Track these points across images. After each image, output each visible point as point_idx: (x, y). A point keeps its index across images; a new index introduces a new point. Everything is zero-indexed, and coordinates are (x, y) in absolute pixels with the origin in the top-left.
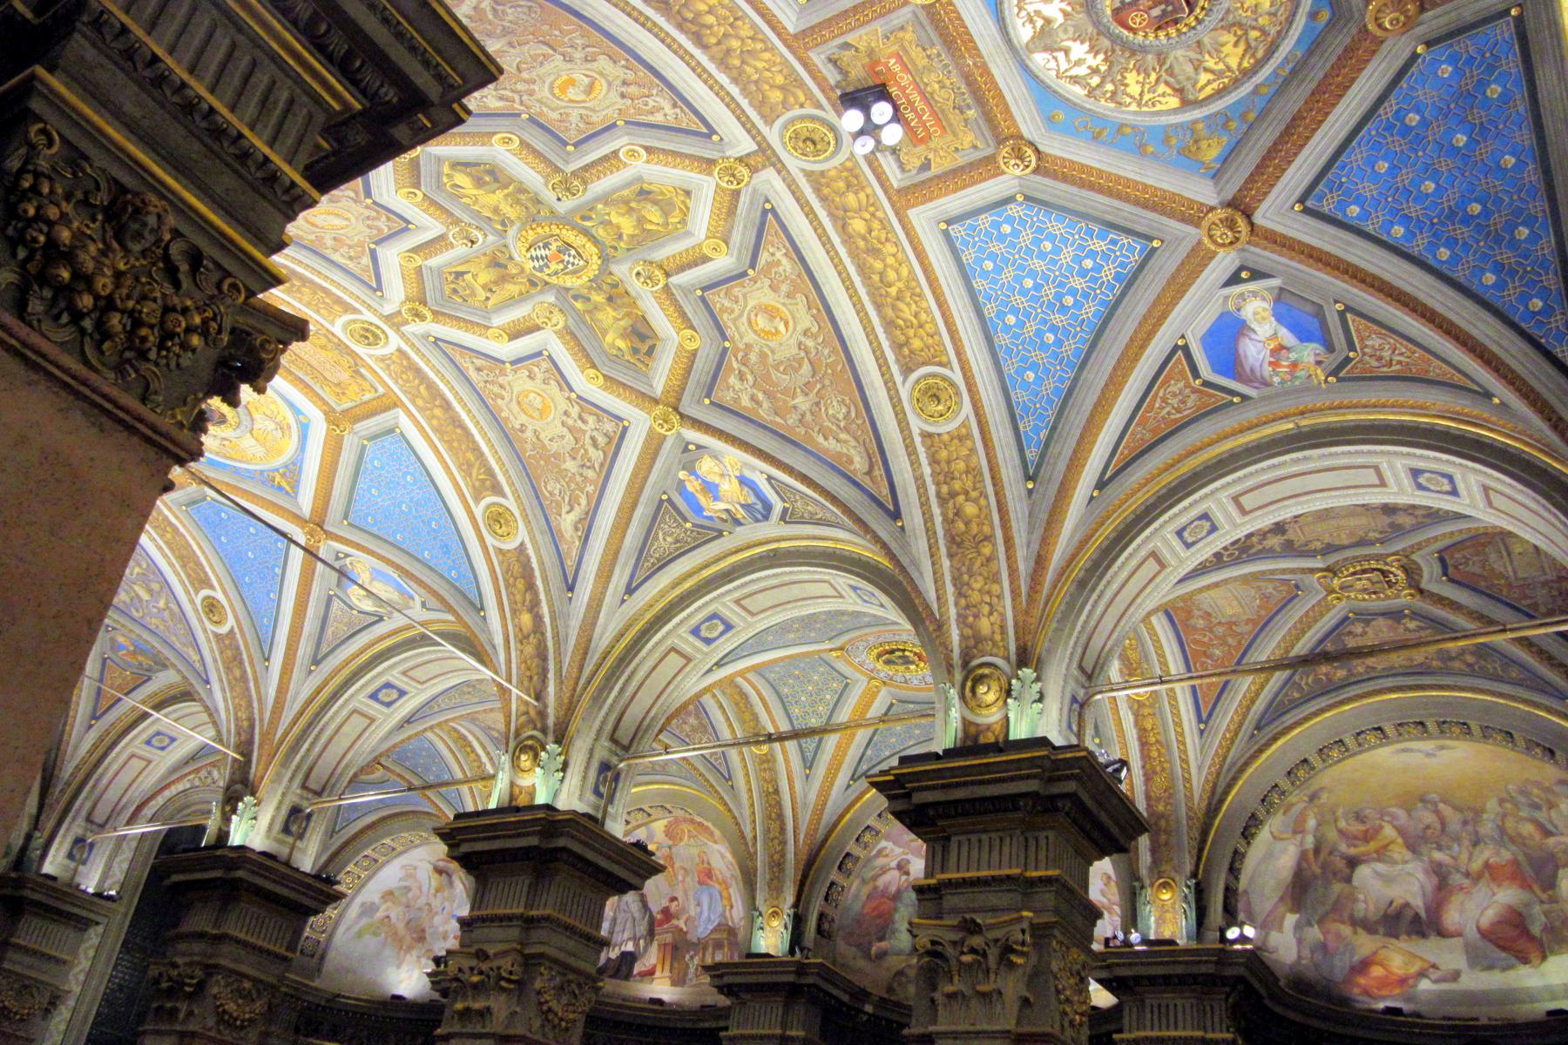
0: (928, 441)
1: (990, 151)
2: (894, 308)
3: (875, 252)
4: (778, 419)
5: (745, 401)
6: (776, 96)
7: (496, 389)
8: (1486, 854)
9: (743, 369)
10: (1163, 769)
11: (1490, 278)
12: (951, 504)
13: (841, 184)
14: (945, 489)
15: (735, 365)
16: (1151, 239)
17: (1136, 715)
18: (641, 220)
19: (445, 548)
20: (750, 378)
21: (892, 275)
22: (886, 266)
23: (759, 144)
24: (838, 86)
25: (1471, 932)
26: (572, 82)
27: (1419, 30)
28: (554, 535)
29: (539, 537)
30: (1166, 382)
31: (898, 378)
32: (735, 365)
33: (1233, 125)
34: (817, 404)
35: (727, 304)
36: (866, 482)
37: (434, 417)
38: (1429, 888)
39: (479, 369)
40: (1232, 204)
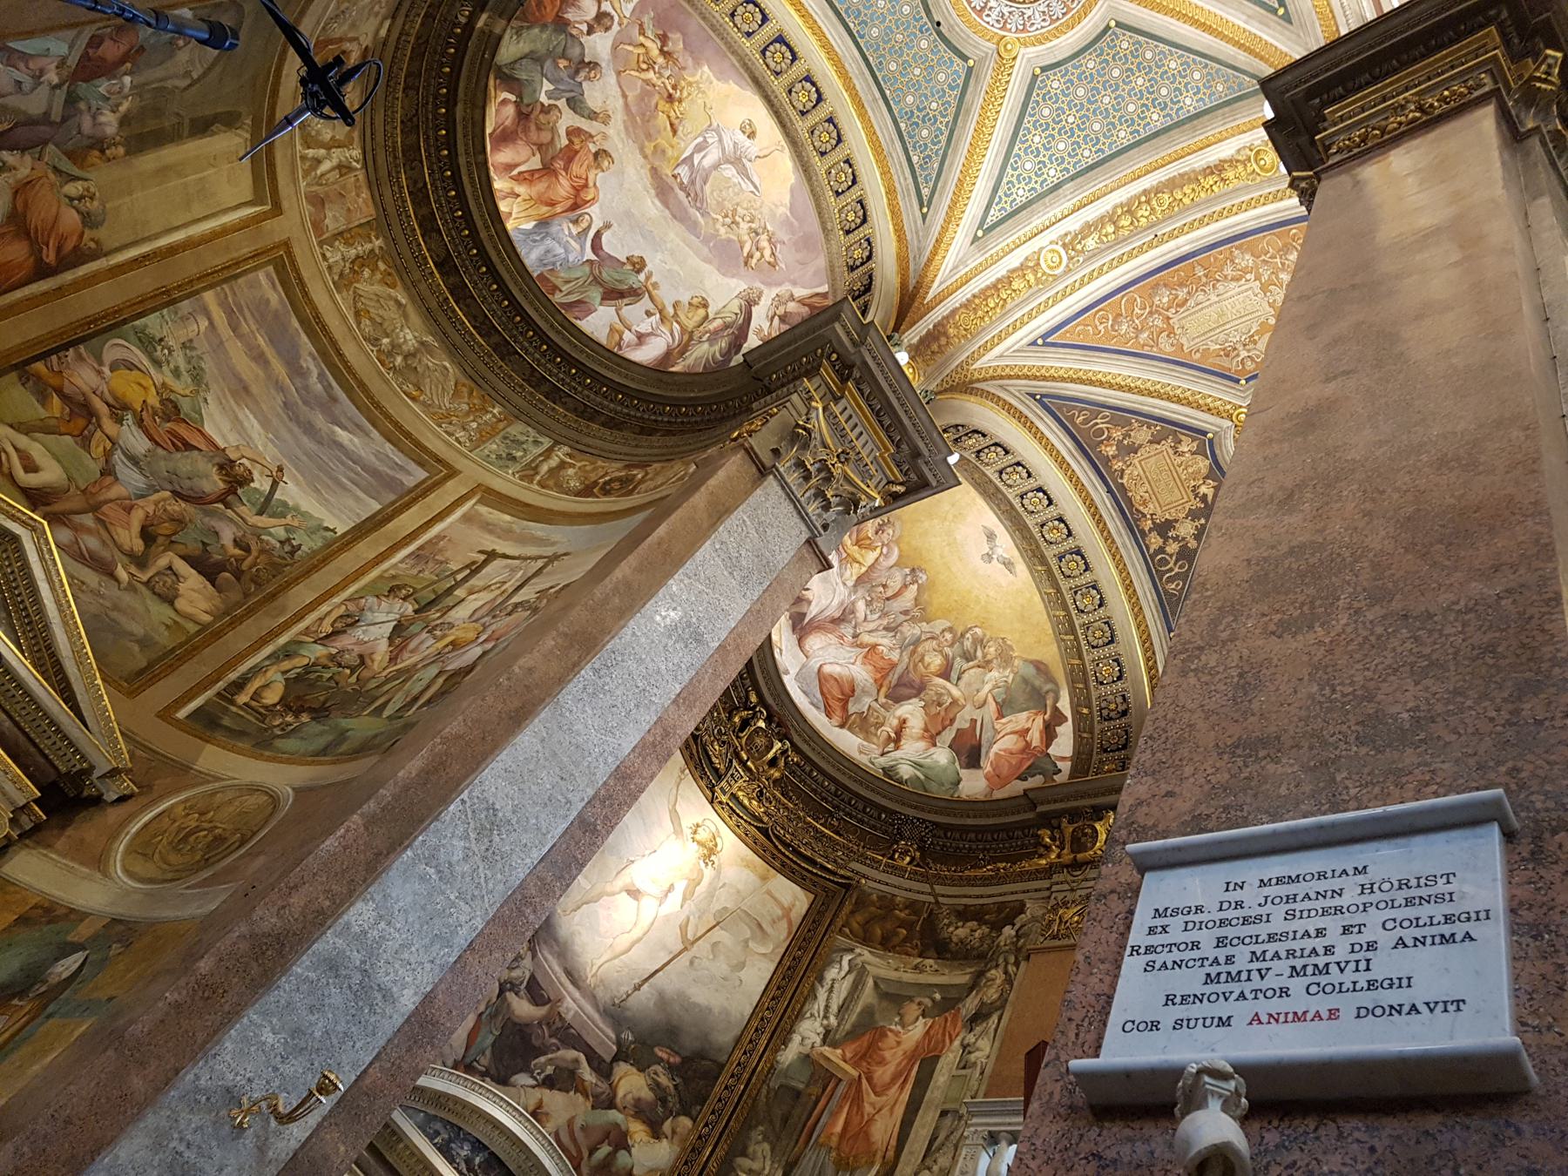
8: (885, 642)
10: (982, 318)
17: (1022, 267)
25: (815, 664)
38: (827, 613)
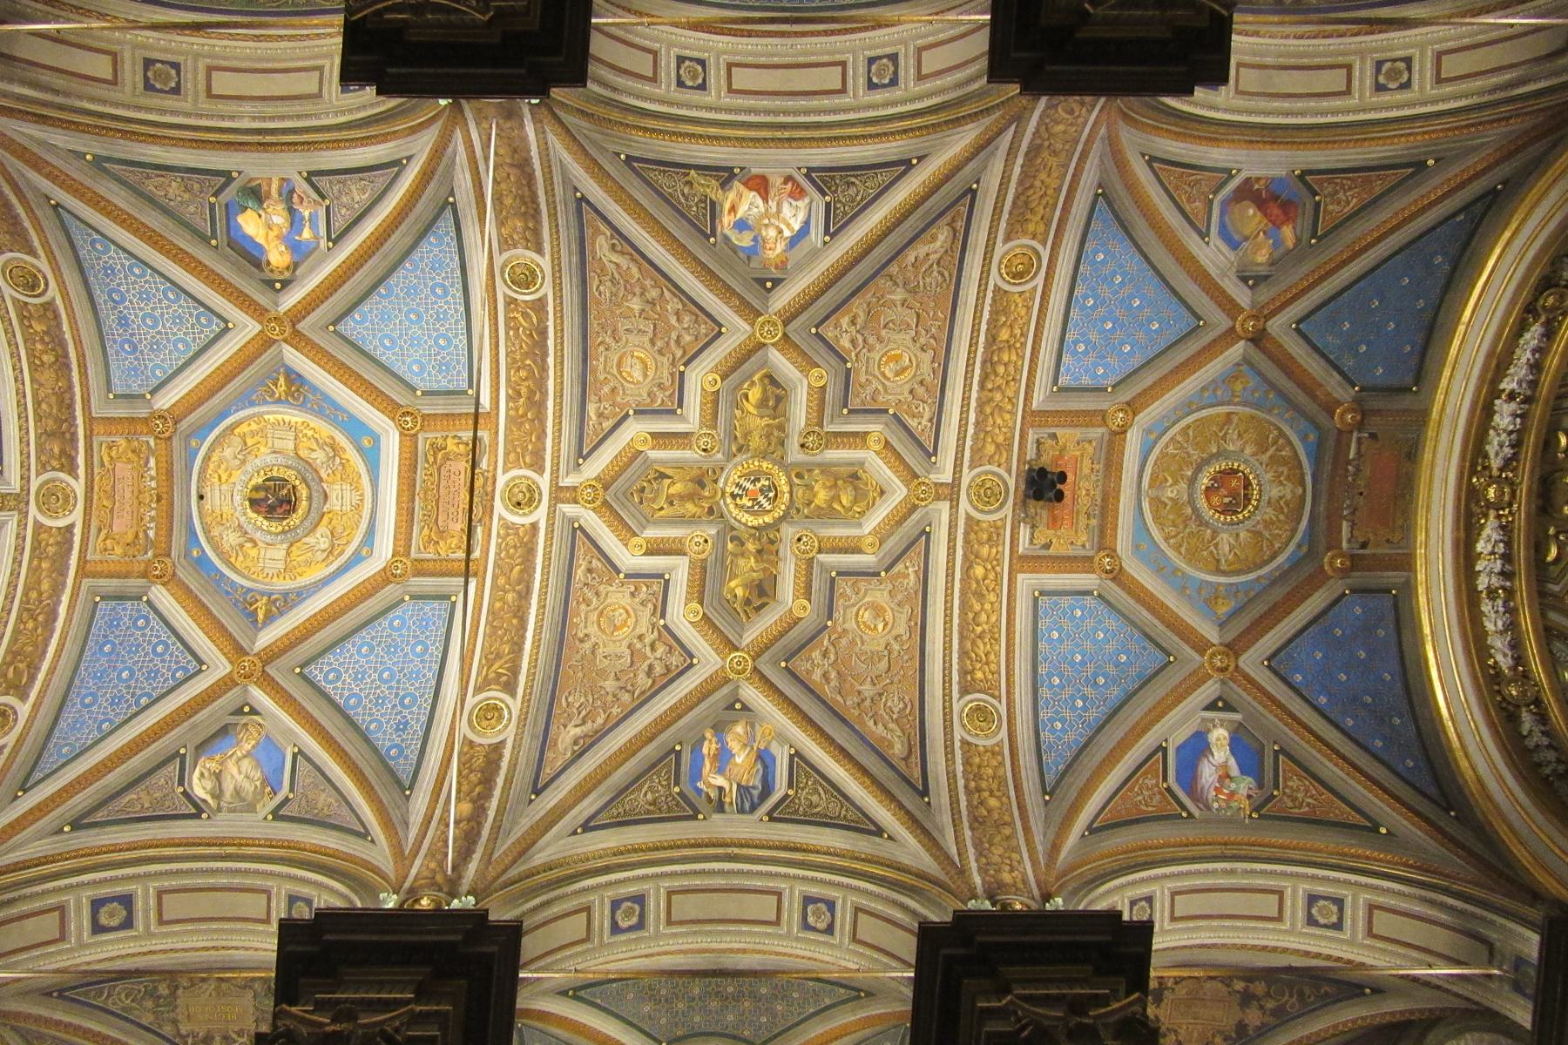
0: (966, 747)
1: (1091, 553)
2: (974, 643)
3: (980, 596)
4: (839, 698)
5: (817, 676)
6: (990, 449)
7: (590, 594)
9: (831, 648)
11: (1379, 743)
12: (976, 795)
13: (985, 536)
14: (973, 784)
15: (826, 642)
16: (1169, 655)
18: (836, 498)
19: (402, 727)
20: (832, 657)
21: (983, 617)
22: (982, 609)
23: (954, 480)
24: (1029, 463)
26: (897, 359)
27: (1349, 581)
28: (545, 741)
29: (527, 739)
30: (1146, 773)
31: (955, 695)
32: (826, 642)
33: (1241, 595)
34: (881, 695)
35: (848, 591)
36: (902, 766)
37: (502, 599)
39: (590, 571)
40: (1228, 646)
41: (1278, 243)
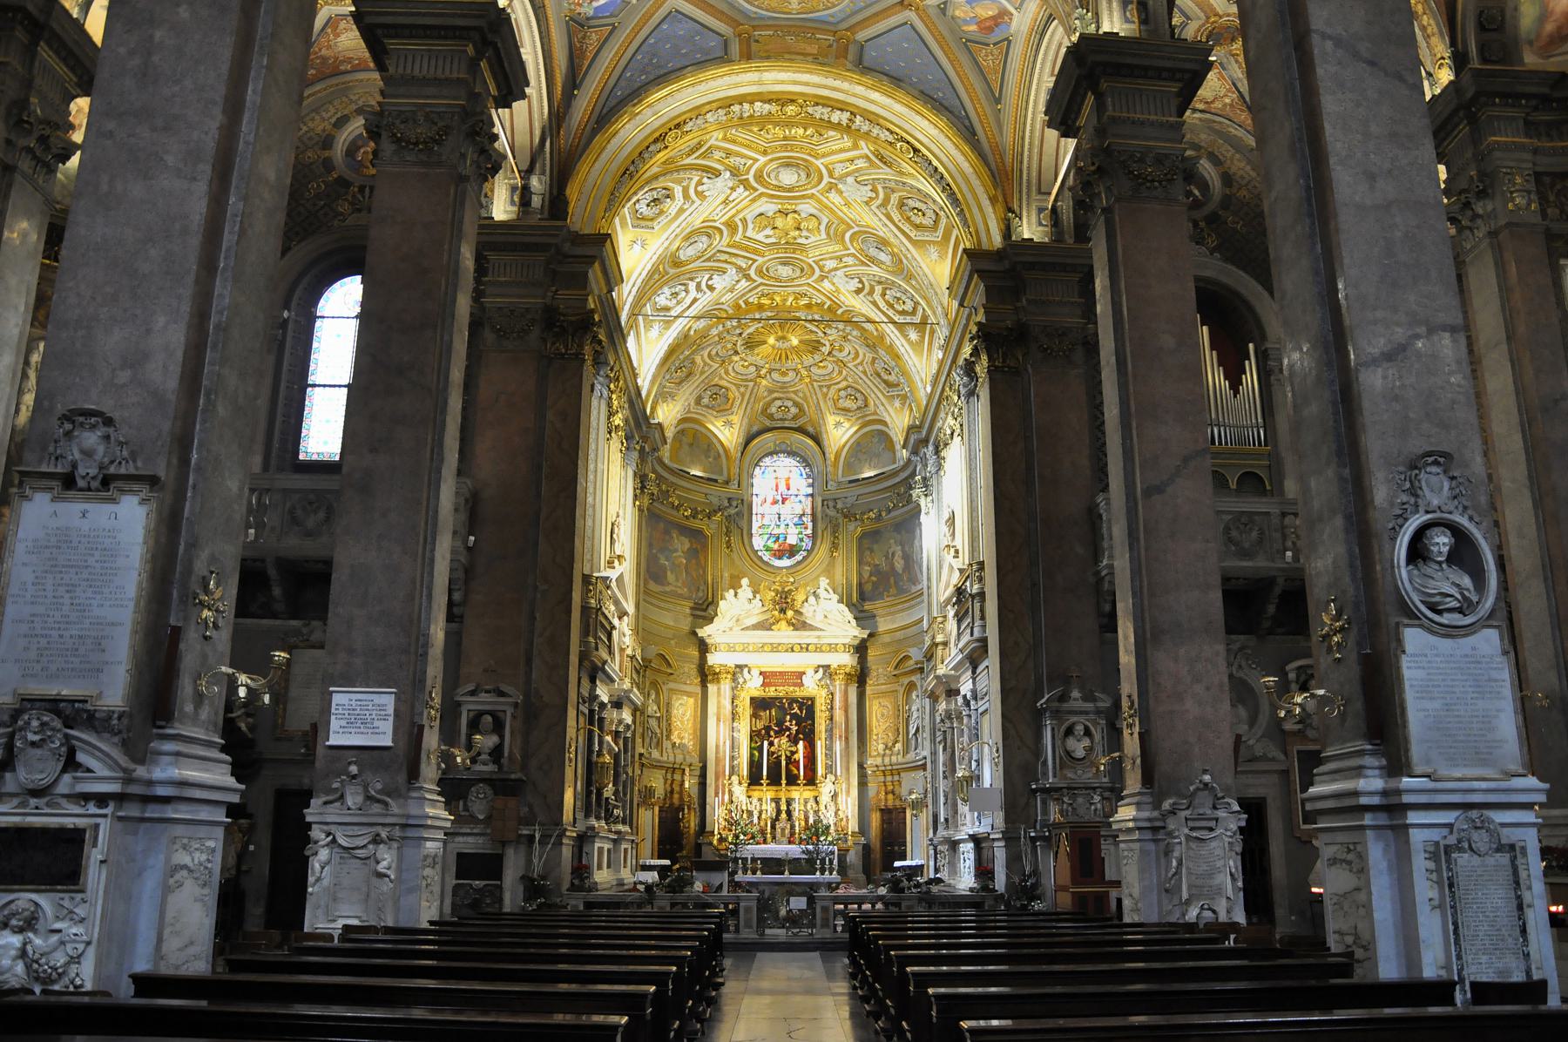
11: (628, 74)
41: (966, 22)
